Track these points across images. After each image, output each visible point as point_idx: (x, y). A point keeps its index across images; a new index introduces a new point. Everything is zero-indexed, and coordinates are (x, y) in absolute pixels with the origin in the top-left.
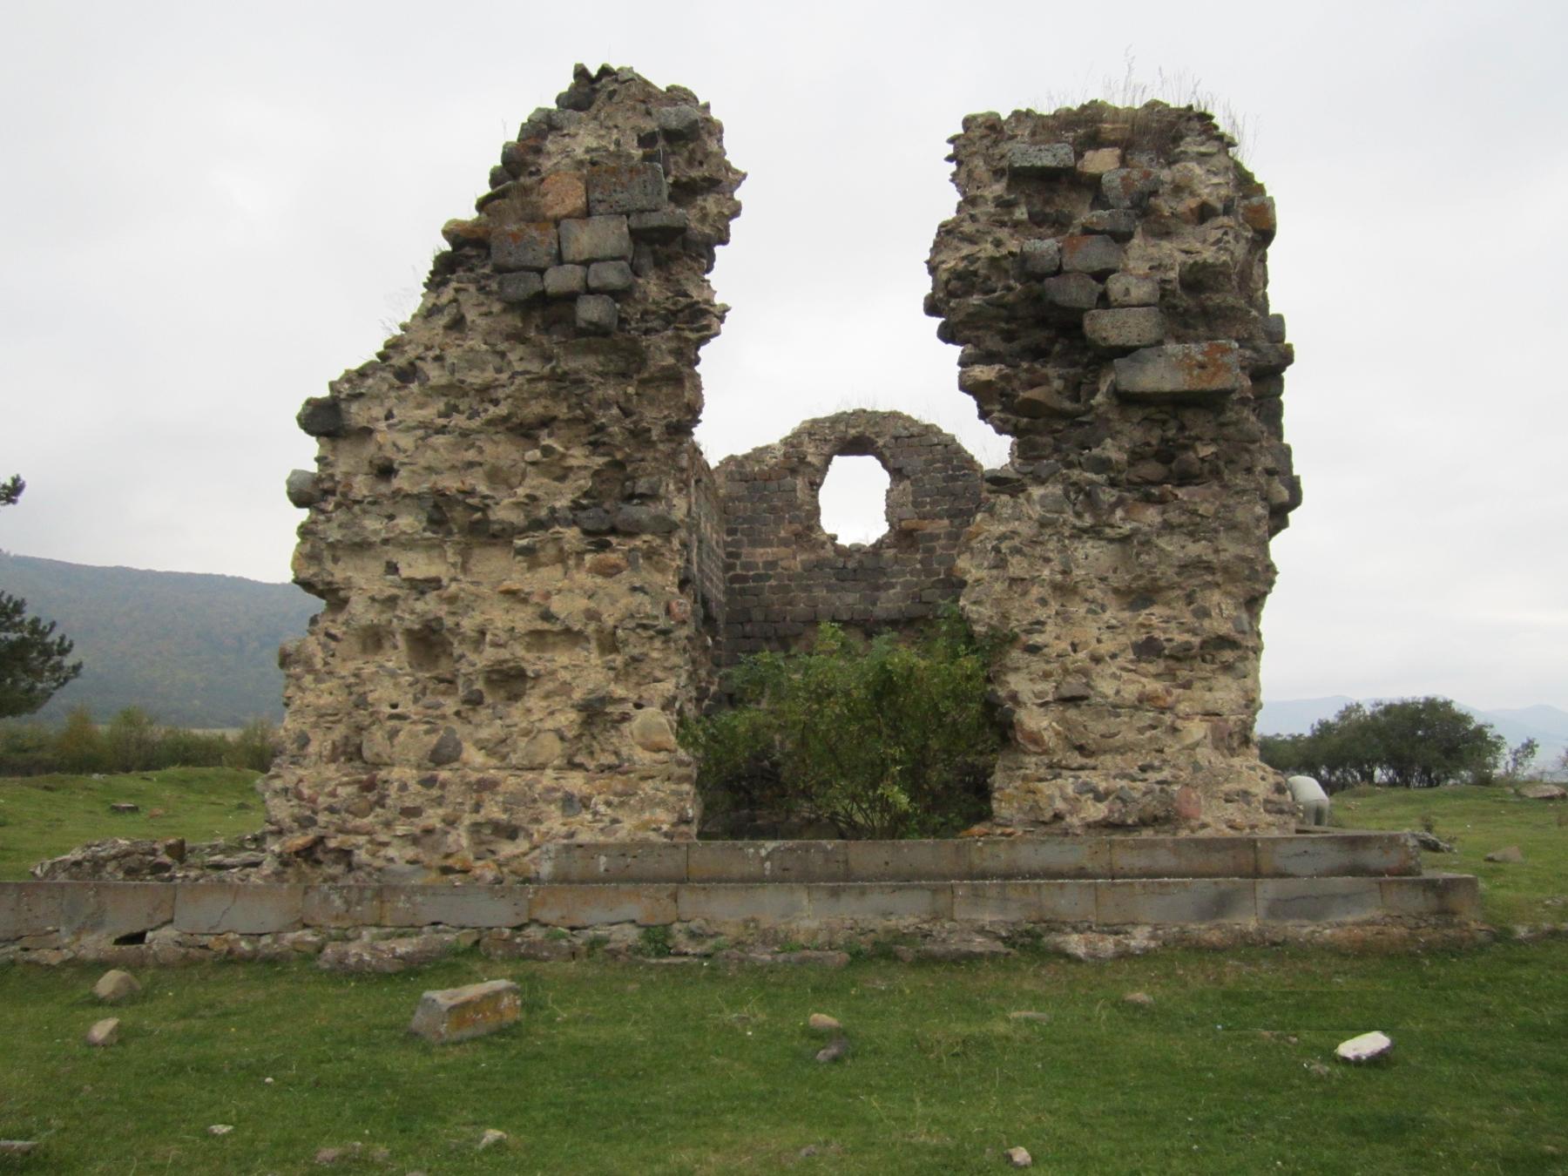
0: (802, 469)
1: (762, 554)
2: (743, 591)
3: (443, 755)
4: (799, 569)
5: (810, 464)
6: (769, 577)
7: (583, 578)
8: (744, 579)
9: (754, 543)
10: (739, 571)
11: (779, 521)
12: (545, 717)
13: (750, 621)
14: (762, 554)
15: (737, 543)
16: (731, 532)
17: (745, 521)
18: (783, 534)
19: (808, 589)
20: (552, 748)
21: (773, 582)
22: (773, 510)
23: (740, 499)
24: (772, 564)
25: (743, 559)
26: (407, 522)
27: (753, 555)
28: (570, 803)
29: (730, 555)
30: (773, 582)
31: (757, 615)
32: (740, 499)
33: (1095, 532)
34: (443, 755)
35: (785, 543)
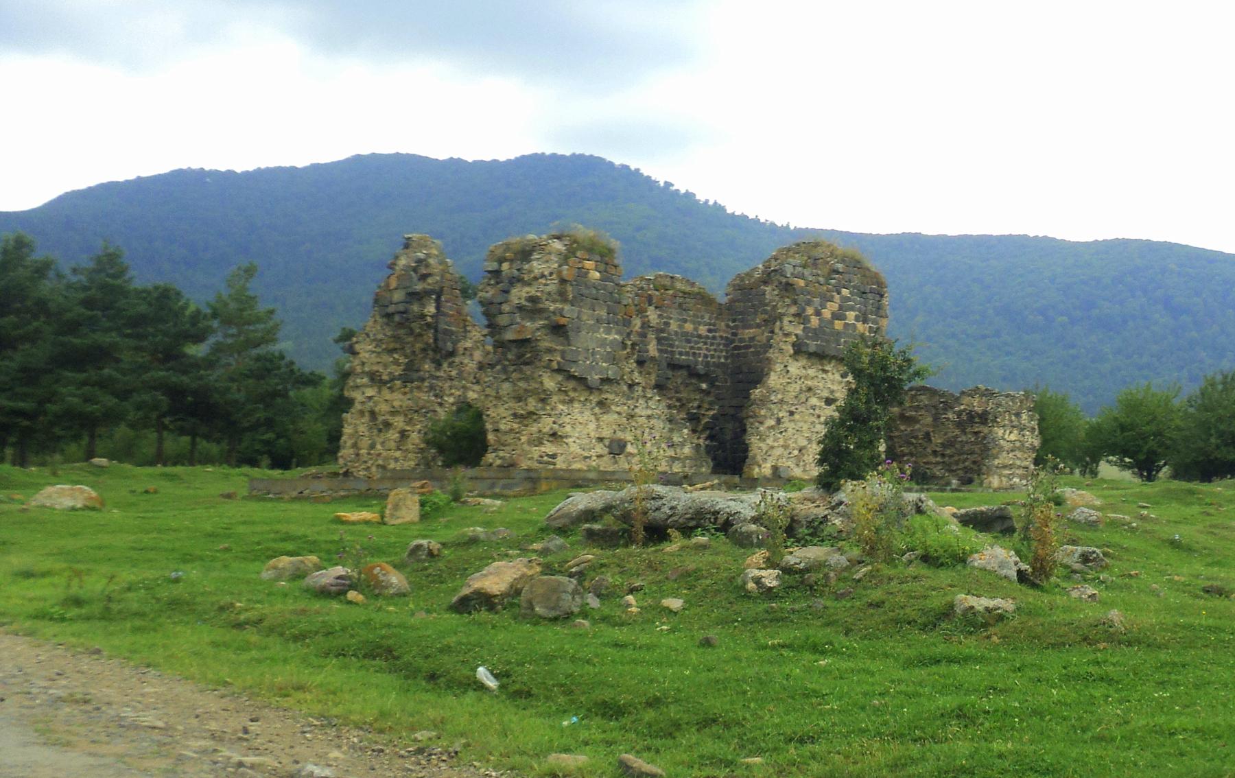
3: (372, 446)
6: (750, 347)
7: (401, 396)
11: (756, 313)
12: (393, 435)
16: (734, 321)
20: (393, 445)
22: (753, 306)
23: (738, 301)
24: (752, 339)
26: (365, 380)
28: (396, 460)
32: (738, 301)
33: (506, 380)
34: (372, 446)
35: (758, 326)
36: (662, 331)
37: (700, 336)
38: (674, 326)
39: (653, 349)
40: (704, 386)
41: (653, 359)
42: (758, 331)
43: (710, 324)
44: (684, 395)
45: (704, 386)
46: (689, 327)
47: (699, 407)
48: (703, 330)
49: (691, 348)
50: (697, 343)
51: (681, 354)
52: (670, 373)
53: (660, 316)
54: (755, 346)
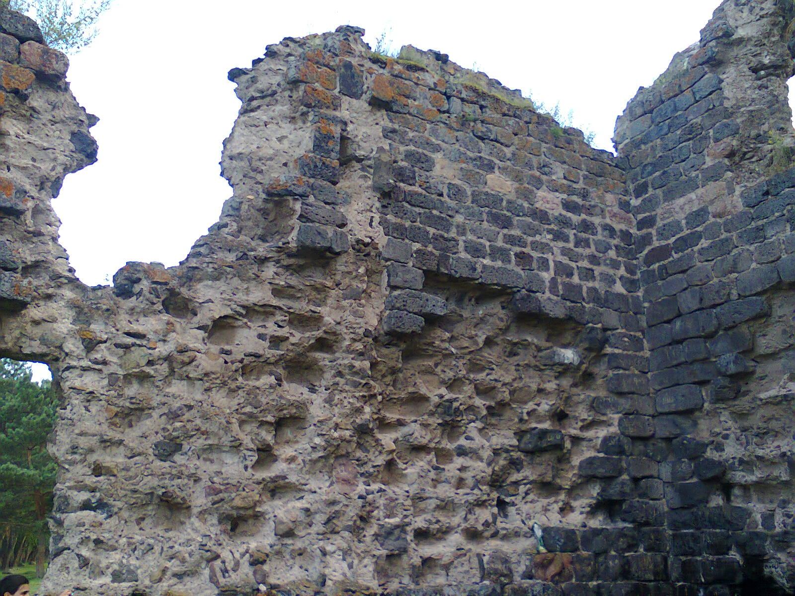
0: (736, 51)
1: (681, 207)
2: (664, 273)
4: (741, 207)
5: (740, 41)
8: (661, 253)
9: (670, 196)
10: (656, 244)
13: (679, 315)
14: (681, 207)
15: (650, 204)
16: (640, 191)
17: (655, 166)
18: (709, 162)
19: (758, 234)
21: (704, 243)
24: (699, 216)
25: (660, 223)
27: (670, 212)
29: (641, 225)
30: (704, 243)
31: (688, 302)
35: (714, 175)
36: (410, 179)
37: (542, 216)
38: (444, 170)
39: (360, 214)
40: (569, 355)
41: (363, 249)
42: (712, 189)
43: (571, 192)
44: (503, 375)
45: (569, 355)
46: (499, 183)
47: (560, 416)
48: (548, 200)
49: (510, 240)
50: (532, 231)
51: (476, 250)
52: (437, 304)
53: (388, 133)
54: (711, 231)
